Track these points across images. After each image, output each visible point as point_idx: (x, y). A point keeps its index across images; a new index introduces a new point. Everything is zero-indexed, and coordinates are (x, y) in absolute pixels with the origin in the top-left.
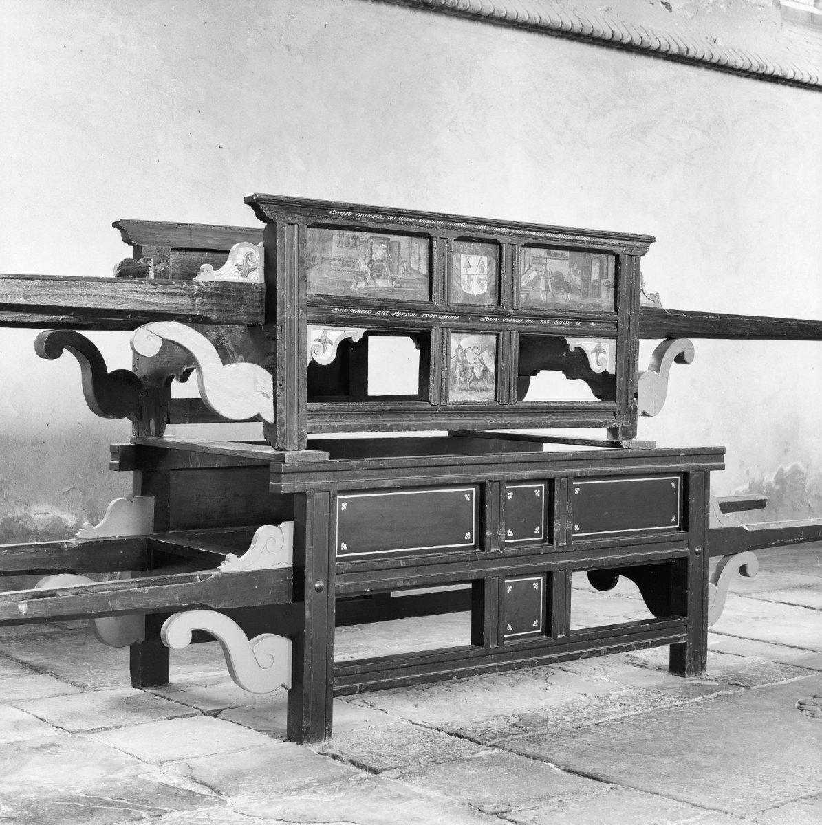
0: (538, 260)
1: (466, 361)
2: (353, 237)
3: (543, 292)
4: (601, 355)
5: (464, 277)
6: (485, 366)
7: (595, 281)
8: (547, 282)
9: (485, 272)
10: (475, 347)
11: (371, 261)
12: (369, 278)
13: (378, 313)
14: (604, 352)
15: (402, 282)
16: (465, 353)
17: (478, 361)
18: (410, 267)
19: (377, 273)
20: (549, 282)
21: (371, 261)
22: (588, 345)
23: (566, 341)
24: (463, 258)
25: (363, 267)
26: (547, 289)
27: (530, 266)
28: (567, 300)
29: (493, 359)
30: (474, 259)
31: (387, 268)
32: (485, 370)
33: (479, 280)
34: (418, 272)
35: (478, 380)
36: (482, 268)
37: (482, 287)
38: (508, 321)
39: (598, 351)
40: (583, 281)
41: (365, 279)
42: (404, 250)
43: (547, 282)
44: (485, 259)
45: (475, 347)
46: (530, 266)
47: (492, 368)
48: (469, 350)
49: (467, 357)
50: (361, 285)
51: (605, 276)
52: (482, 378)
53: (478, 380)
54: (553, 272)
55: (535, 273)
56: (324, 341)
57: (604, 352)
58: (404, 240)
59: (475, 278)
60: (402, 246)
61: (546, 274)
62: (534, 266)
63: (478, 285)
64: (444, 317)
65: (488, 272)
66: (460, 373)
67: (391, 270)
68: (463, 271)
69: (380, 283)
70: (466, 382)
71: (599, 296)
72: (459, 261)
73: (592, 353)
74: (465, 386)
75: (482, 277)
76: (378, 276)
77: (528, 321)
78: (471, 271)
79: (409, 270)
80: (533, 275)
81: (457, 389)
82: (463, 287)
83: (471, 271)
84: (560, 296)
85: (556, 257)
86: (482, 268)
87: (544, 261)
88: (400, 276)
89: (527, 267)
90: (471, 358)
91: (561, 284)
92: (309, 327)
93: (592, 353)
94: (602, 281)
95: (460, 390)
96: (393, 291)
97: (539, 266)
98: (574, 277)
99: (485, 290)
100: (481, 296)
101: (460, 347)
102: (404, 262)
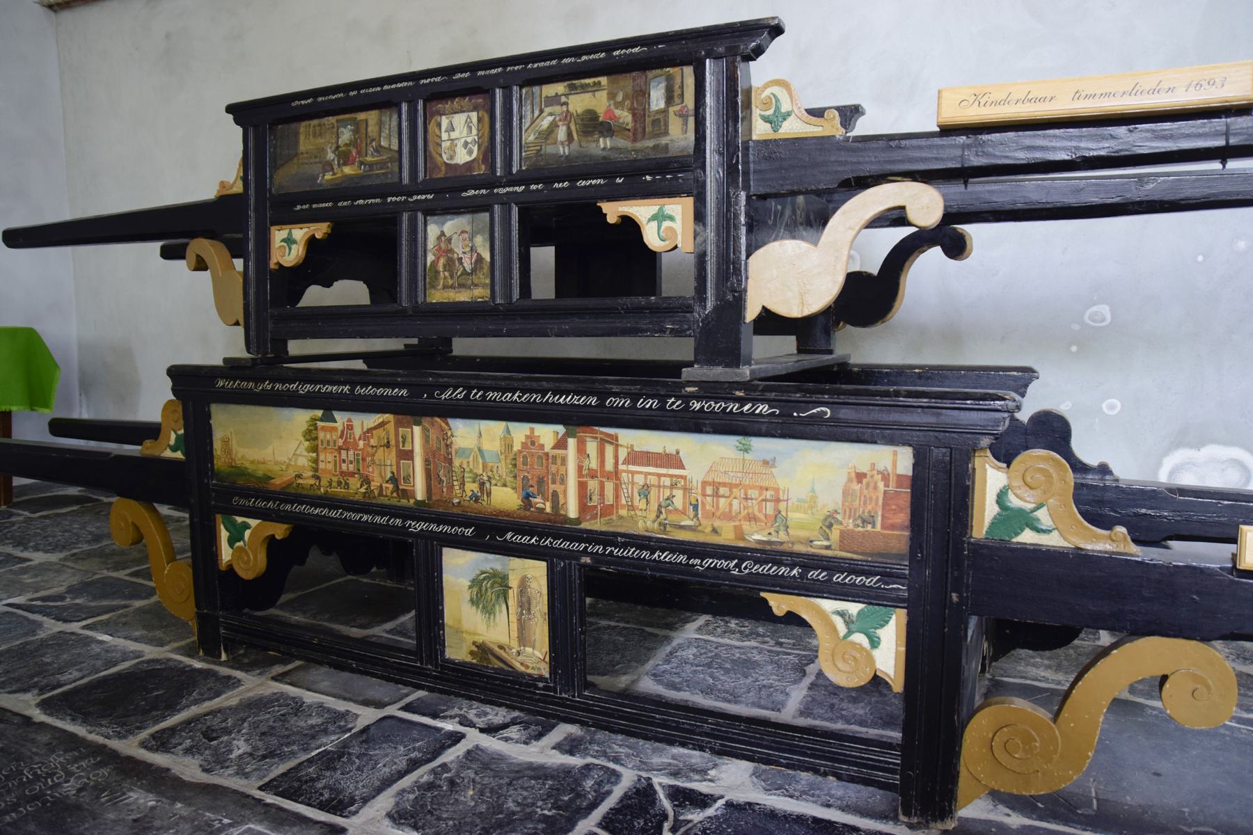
0: (554, 100)
1: (451, 251)
2: (320, 125)
3: (562, 143)
4: (666, 224)
5: (445, 145)
6: (479, 254)
7: (658, 112)
8: (569, 128)
9: (474, 131)
10: (463, 232)
11: (338, 147)
12: (335, 167)
13: (340, 204)
14: (671, 218)
15: (371, 165)
16: (449, 240)
17: (468, 249)
18: (381, 146)
19: (345, 158)
20: (573, 127)
21: (338, 147)
22: (641, 210)
23: (600, 208)
24: (445, 121)
25: (331, 156)
26: (570, 134)
27: (541, 111)
28: (604, 149)
29: (488, 245)
30: (459, 120)
31: (354, 152)
32: (480, 259)
33: (466, 144)
34: (389, 149)
35: (469, 274)
36: (470, 128)
37: (470, 152)
38: (502, 191)
39: (659, 217)
40: (634, 115)
41: (332, 169)
42: (372, 129)
43: (569, 128)
44: (474, 115)
45: (463, 232)
46: (541, 111)
47: (487, 256)
48: (455, 236)
49: (453, 246)
50: (328, 176)
51: (677, 100)
52: (474, 270)
53: (469, 274)
54: (580, 111)
55: (550, 118)
56: (289, 241)
57: (671, 218)
58: (372, 116)
59: (460, 144)
60: (370, 122)
61: (567, 116)
62: (547, 110)
63: (465, 151)
64: (415, 197)
65: (478, 130)
66: (444, 266)
67: (359, 153)
68: (444, 136)
69: (348, 170)
70: (452, 277)
71: (666, 133)
72: (439, 125)
73: (649, 220)
74: (450, 282)
75: (469, 140)
76: (345, 164)
77: (533, 187)
78: (454, 135)
79: (379, 149)
80: (546, 122)
81: (440, 287)
82: (445, 157)
83: (454, 135)
84: (594, 145)
85: (584, 89)
86: (470, 128)
87: (563, 99)
88: (369, 159)
89: (537, 113)
90: (459, 248)
91: (592, 124)
92: (273, 229)
93: (649, 220)
94: (671, 109)
95: (445, 287)
96: (361, 177)
97: (557, 109)
98: (618, 112)
99: (475, 155)
100: (469, 165)
101: (443, 234)
102: (373, 140)
